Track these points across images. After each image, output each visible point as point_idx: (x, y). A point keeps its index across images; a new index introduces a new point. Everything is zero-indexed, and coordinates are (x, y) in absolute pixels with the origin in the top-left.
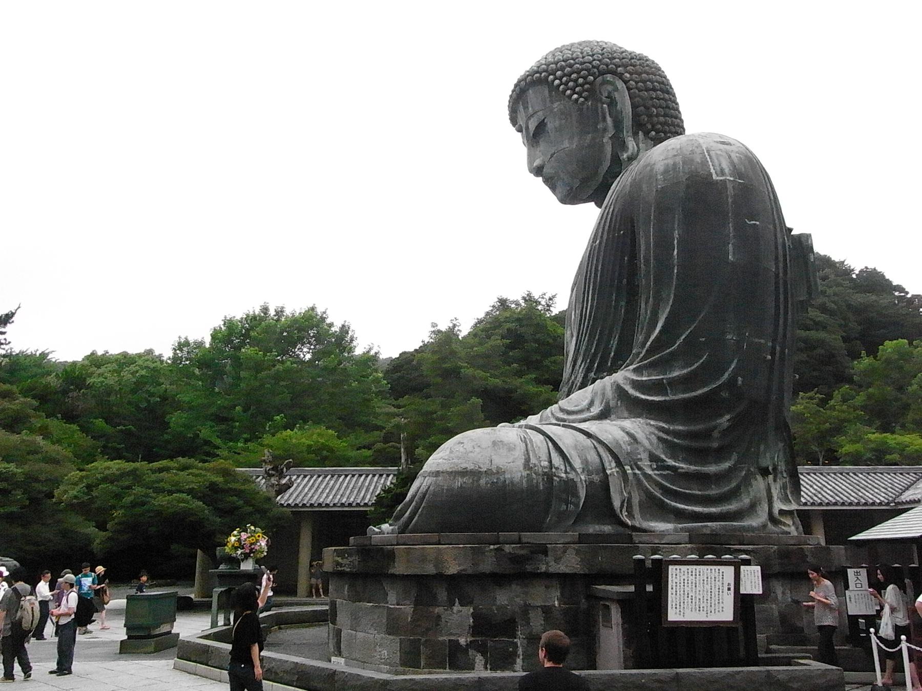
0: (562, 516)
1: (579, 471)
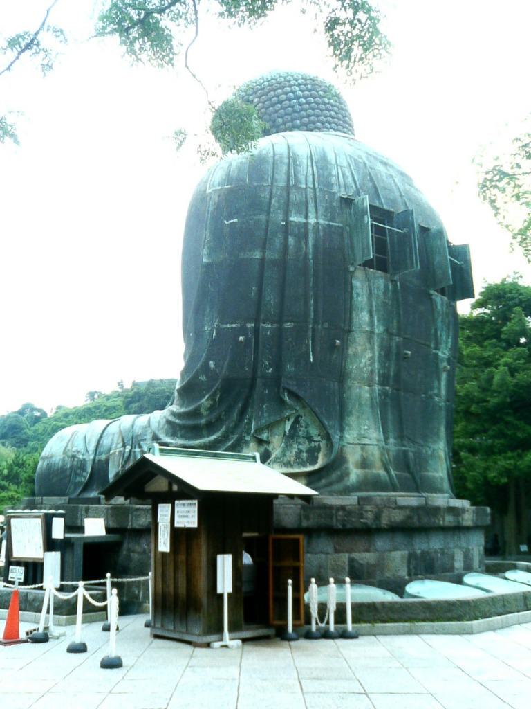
0: (76, 485)
1: (90, 453)
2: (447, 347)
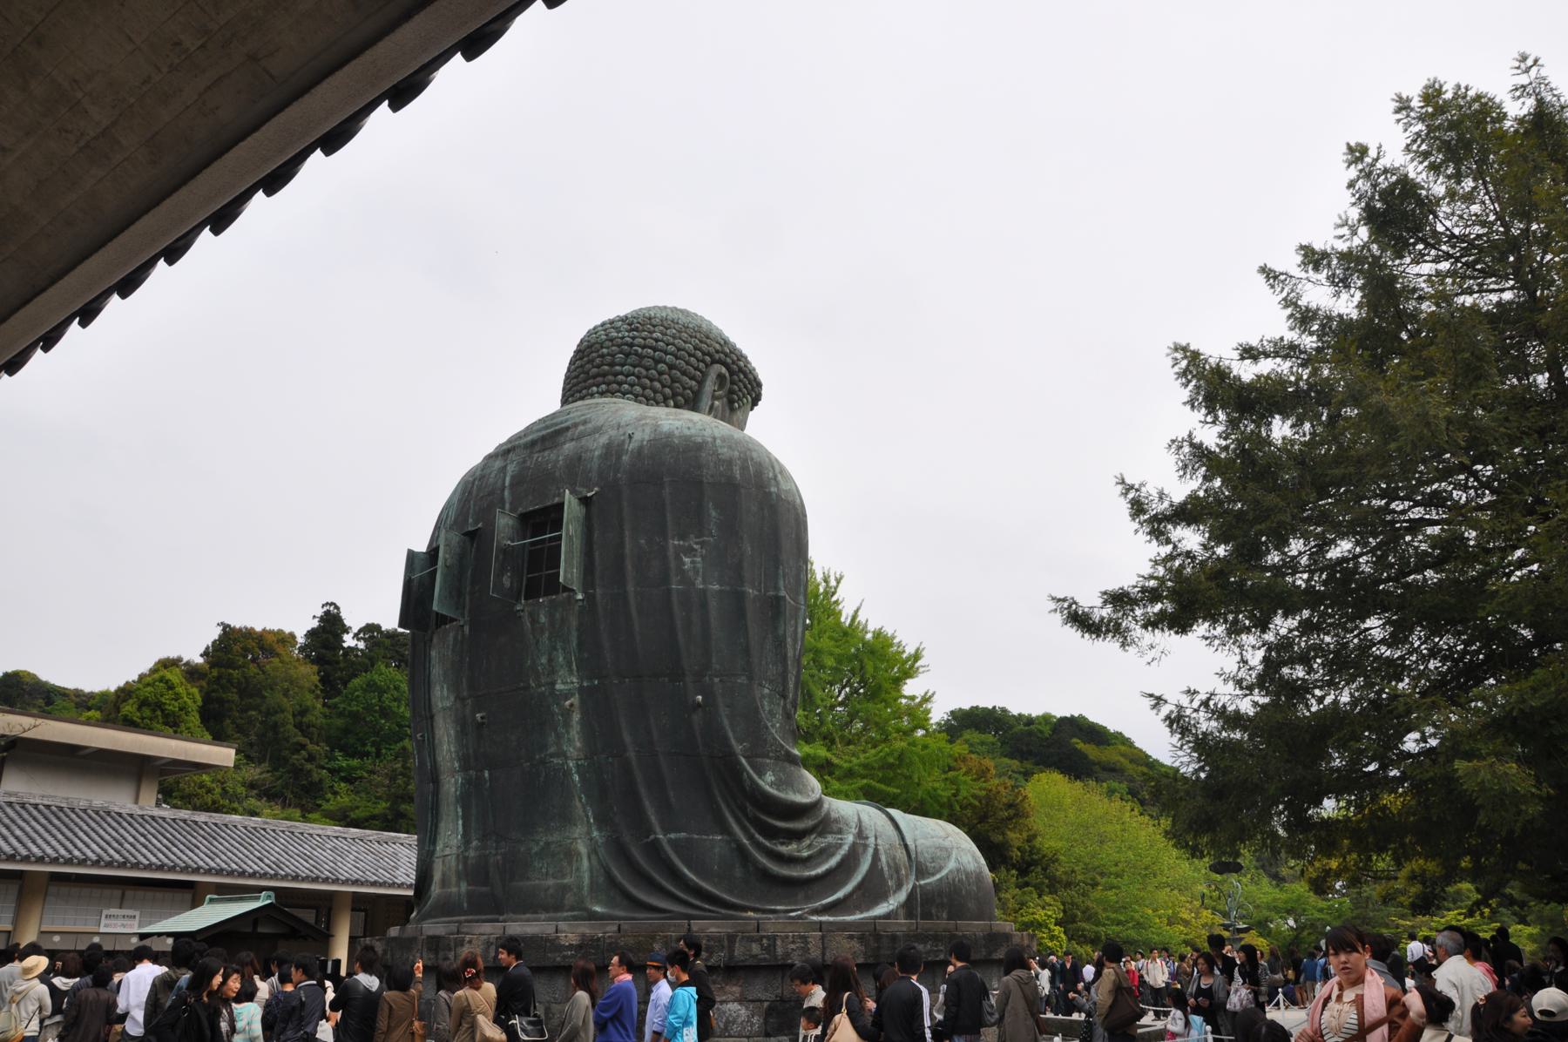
2: (571, 671)
